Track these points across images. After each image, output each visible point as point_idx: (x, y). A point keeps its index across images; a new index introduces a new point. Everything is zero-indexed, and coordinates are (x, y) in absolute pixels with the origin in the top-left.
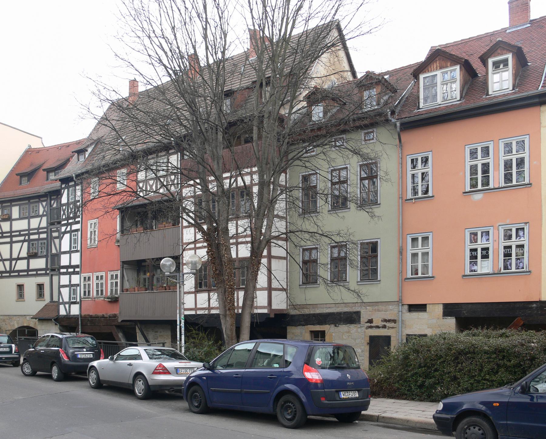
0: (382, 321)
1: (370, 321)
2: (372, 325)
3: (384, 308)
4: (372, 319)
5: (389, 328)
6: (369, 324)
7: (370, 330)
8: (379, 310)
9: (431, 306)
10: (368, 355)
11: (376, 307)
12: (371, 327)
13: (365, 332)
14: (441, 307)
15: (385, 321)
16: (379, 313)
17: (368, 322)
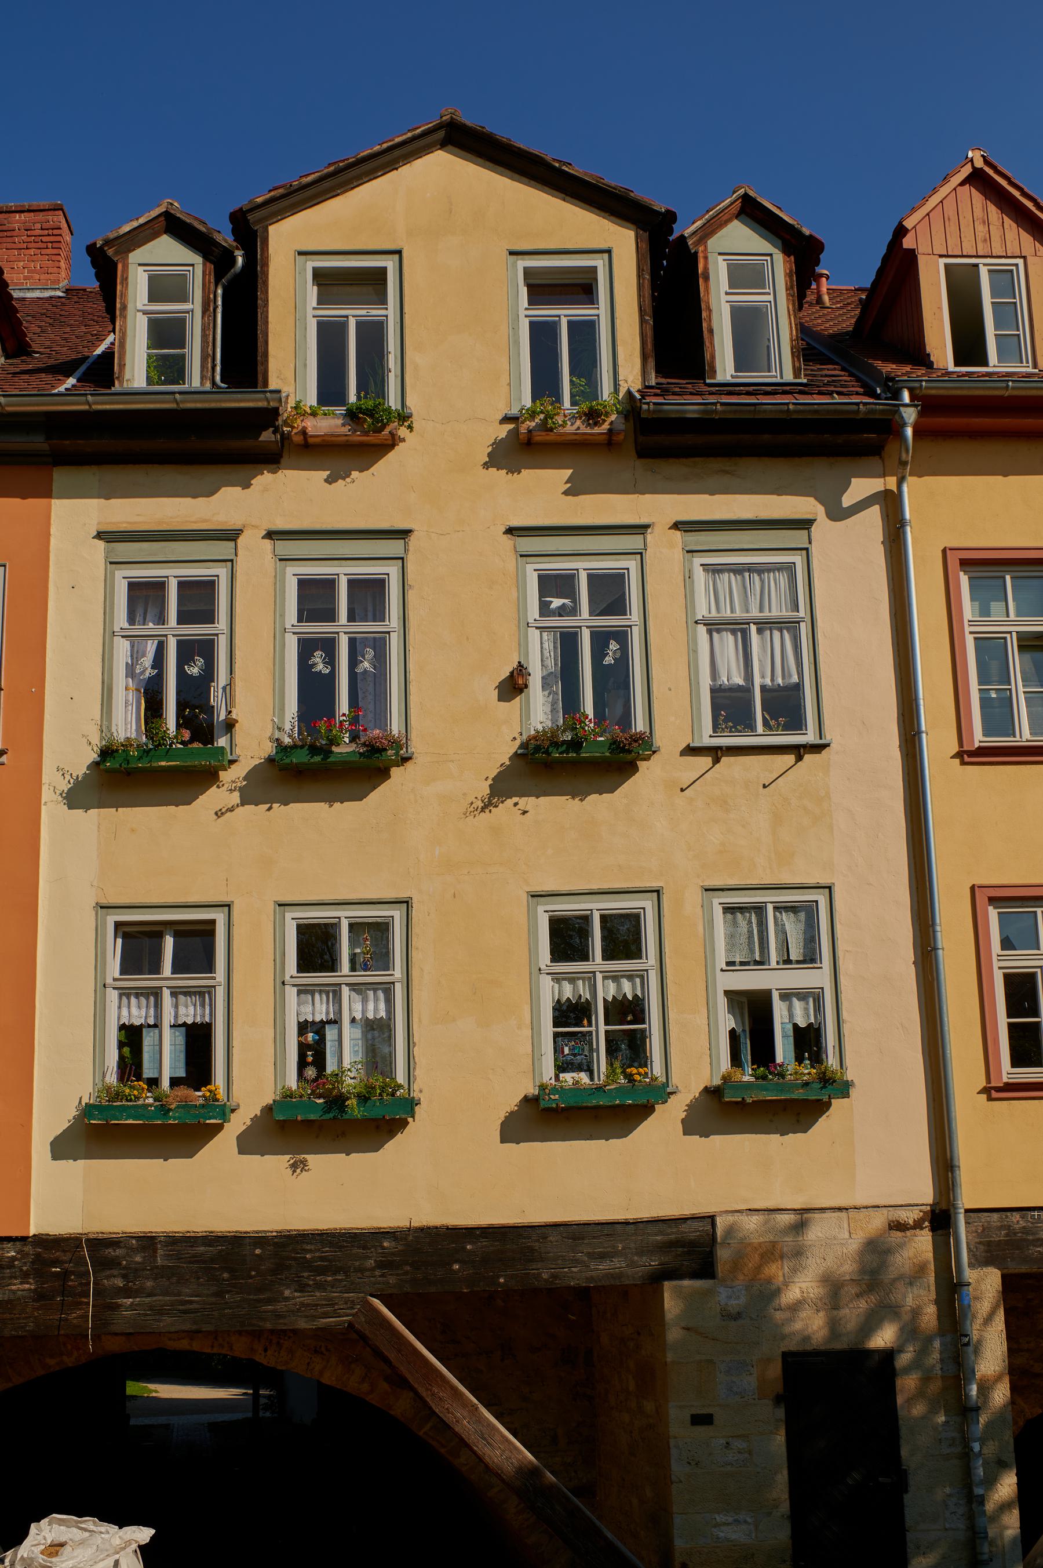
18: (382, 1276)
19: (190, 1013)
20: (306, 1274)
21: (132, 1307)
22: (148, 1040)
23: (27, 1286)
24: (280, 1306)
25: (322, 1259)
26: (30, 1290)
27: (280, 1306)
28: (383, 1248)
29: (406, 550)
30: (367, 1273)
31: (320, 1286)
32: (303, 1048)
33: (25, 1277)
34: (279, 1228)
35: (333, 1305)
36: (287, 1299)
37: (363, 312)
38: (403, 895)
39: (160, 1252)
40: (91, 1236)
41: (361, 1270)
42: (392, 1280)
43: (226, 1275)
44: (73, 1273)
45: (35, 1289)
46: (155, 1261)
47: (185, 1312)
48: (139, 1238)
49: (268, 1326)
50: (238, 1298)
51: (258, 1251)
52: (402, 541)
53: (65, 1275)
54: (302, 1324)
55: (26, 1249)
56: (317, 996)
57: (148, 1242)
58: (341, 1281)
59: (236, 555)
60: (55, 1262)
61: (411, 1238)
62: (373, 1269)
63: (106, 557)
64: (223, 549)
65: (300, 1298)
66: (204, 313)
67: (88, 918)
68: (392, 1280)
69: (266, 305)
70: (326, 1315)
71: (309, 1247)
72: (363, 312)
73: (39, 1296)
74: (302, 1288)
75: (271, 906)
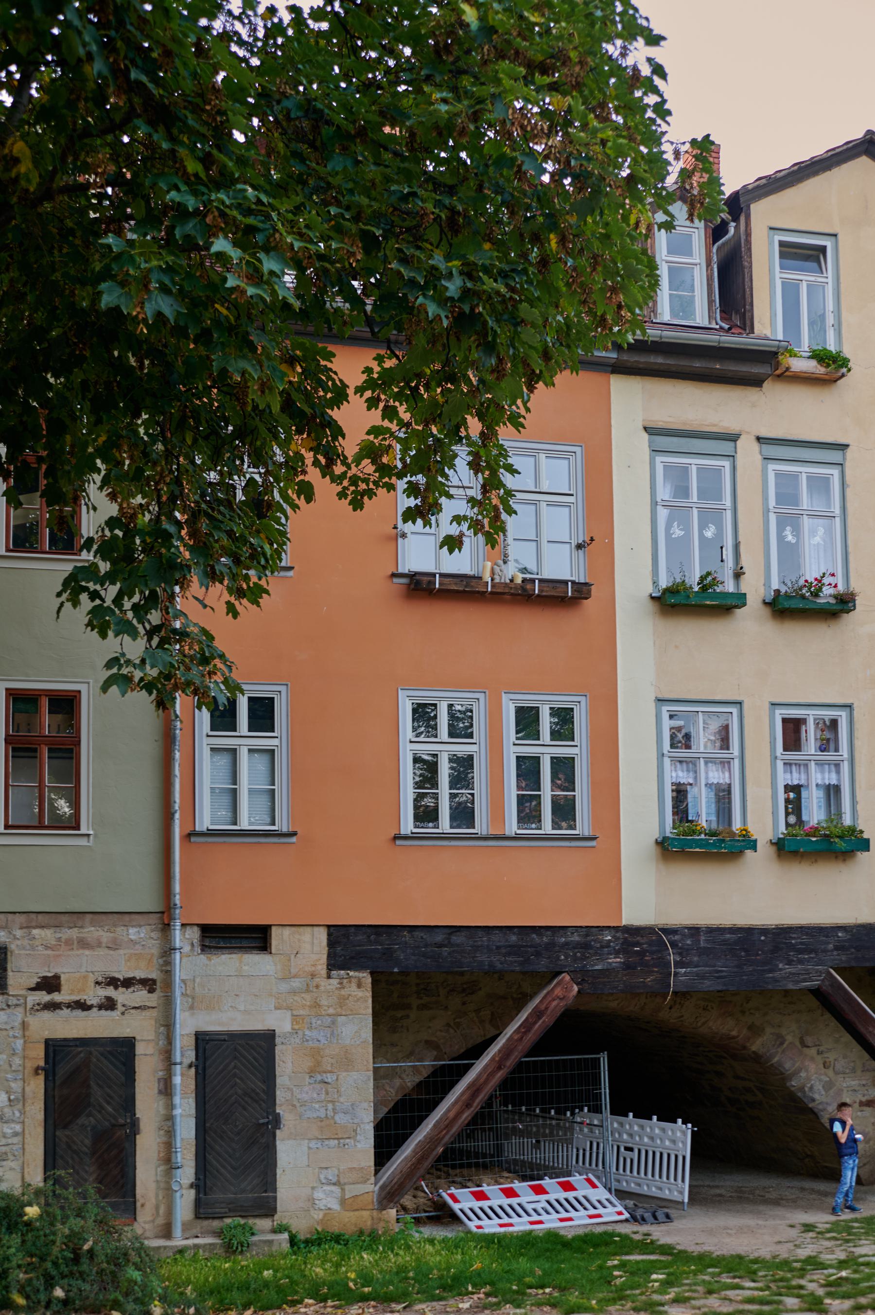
0: (98, 983)
1: (50, 984)
2: (57, 997)
3: (105, 936)
4: (57, 977)
5: (127, 1008)
6: (44, 997)
7: (46, 1015)
8: (83, 944)
9: (287, 931)
10: (41, 1116)
11: (74, 933)
12: (53, 1006)
13: (24, 1026)
14: (322, 935)
15: (113, 982)
16: (87, 952)
17: (38, 987)
18: (838, 955)
19: (717, 776)
20: (792, 953)
21: (685, 974)
22: (692, 793)
23: (618, 960)
24: (777, 974)
25: (801, 943)
26: (620, 962)
27: (777, 974)
28: (839, 937)
29: (844, 459)
30: (829, 953)
31: (801, 962)
32: (787, 801)
33: (617, 953)
34: (777, 923)
35: (809, 974)
36: (781, 970)
37: (812, 279)
38: (848, 701)
39: (703, 938)
40: (660, 926)
41: (825, 951)
42: (844, 958)
43: (743, 954)
44: (647, 951)
45: (623, 963)
46: (699, 944)
47: (718, 978)
48: (689, 928)
49: (770, 987)
50: (751, 969)
51: (763, 938)
52: (841, 452)
53: (642, 953)
54: (791, 986)
55: (618, 935)
56: (794, 767)
57: (695, 931)
58: (813, 958)
59: (736, 452)
60: (637, 944)
61: (854, 931)
62: (832, 951)
63: (650, 446)
64: (725, 447)
65: (789, 969)
66: (707, 267)
67: (652, 706)
68: (844, 958)
69: (751, 267)
70: (805, 981)
71: (794, 936)
72: (812, 279)
73: (627, 967)
74: (790, 962)
75: (767, 705)
